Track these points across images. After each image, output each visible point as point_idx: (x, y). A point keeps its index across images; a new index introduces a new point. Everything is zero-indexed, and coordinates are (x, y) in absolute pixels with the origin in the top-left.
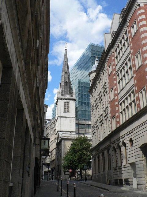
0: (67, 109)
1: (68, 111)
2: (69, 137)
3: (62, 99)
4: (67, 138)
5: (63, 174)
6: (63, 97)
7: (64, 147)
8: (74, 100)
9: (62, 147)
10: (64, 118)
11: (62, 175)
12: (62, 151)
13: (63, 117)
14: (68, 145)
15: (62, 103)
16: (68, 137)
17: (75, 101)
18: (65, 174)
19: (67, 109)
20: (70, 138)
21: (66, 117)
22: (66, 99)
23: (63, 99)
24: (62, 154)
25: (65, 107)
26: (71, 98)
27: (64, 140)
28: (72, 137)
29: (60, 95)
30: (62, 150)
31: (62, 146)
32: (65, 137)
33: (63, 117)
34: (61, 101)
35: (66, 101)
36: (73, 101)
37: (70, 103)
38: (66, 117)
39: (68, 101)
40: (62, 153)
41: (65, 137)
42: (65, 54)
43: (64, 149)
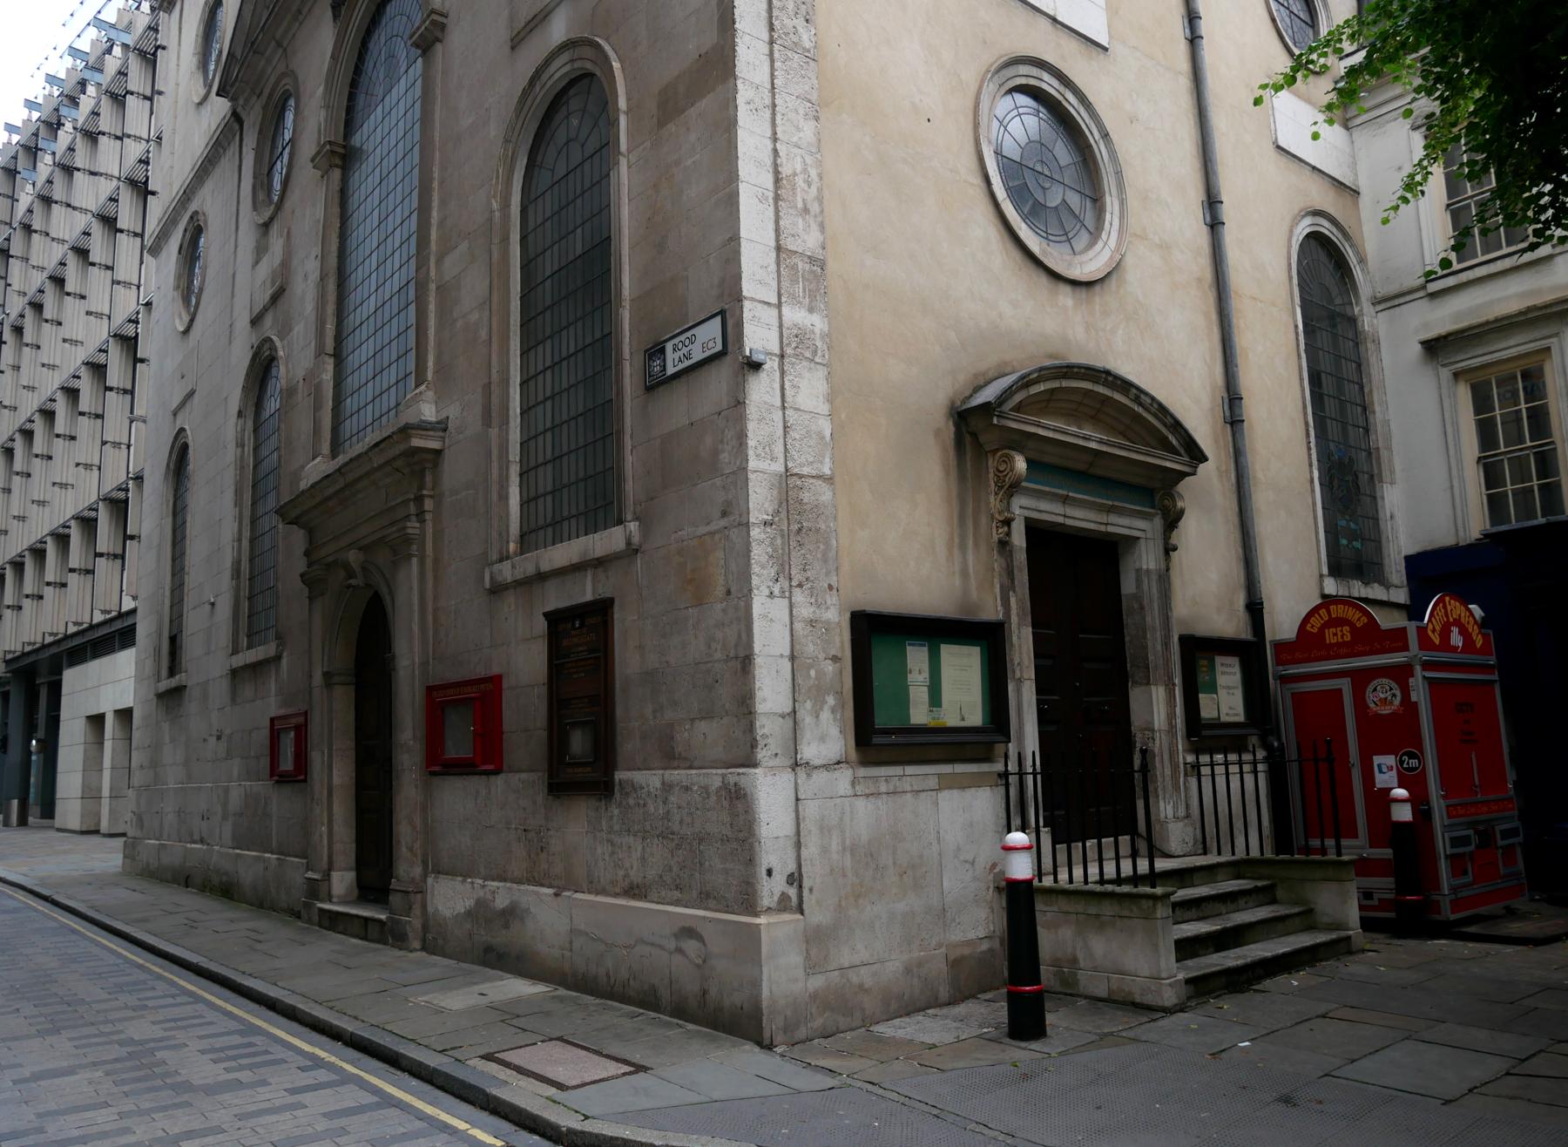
5: (828, 736)
11: (771, 796)
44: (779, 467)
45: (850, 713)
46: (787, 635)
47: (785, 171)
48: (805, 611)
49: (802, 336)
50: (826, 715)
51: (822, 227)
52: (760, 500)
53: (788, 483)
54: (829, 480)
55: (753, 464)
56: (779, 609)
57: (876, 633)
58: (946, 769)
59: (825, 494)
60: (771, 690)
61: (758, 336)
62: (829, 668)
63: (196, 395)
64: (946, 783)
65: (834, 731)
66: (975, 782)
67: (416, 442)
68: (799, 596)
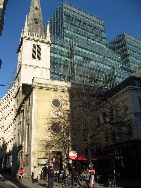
1: (39, 58)
2: (47, 84)
3: (29, 39)
4: (44, 86)
6: (31, 37)
7: (36, 105)
8: (47, 43)
10: (32, 68)
13: (30, 66)
16: (45, 84)
21: (35, 67)
22: (35, 41)
23: (32, 40)
25: (34, 52)
26: (43, 40)
29: (27, 34)
34: (28, 41)
37: (41, 47)
39: (39, 44)
41: (40, 84)
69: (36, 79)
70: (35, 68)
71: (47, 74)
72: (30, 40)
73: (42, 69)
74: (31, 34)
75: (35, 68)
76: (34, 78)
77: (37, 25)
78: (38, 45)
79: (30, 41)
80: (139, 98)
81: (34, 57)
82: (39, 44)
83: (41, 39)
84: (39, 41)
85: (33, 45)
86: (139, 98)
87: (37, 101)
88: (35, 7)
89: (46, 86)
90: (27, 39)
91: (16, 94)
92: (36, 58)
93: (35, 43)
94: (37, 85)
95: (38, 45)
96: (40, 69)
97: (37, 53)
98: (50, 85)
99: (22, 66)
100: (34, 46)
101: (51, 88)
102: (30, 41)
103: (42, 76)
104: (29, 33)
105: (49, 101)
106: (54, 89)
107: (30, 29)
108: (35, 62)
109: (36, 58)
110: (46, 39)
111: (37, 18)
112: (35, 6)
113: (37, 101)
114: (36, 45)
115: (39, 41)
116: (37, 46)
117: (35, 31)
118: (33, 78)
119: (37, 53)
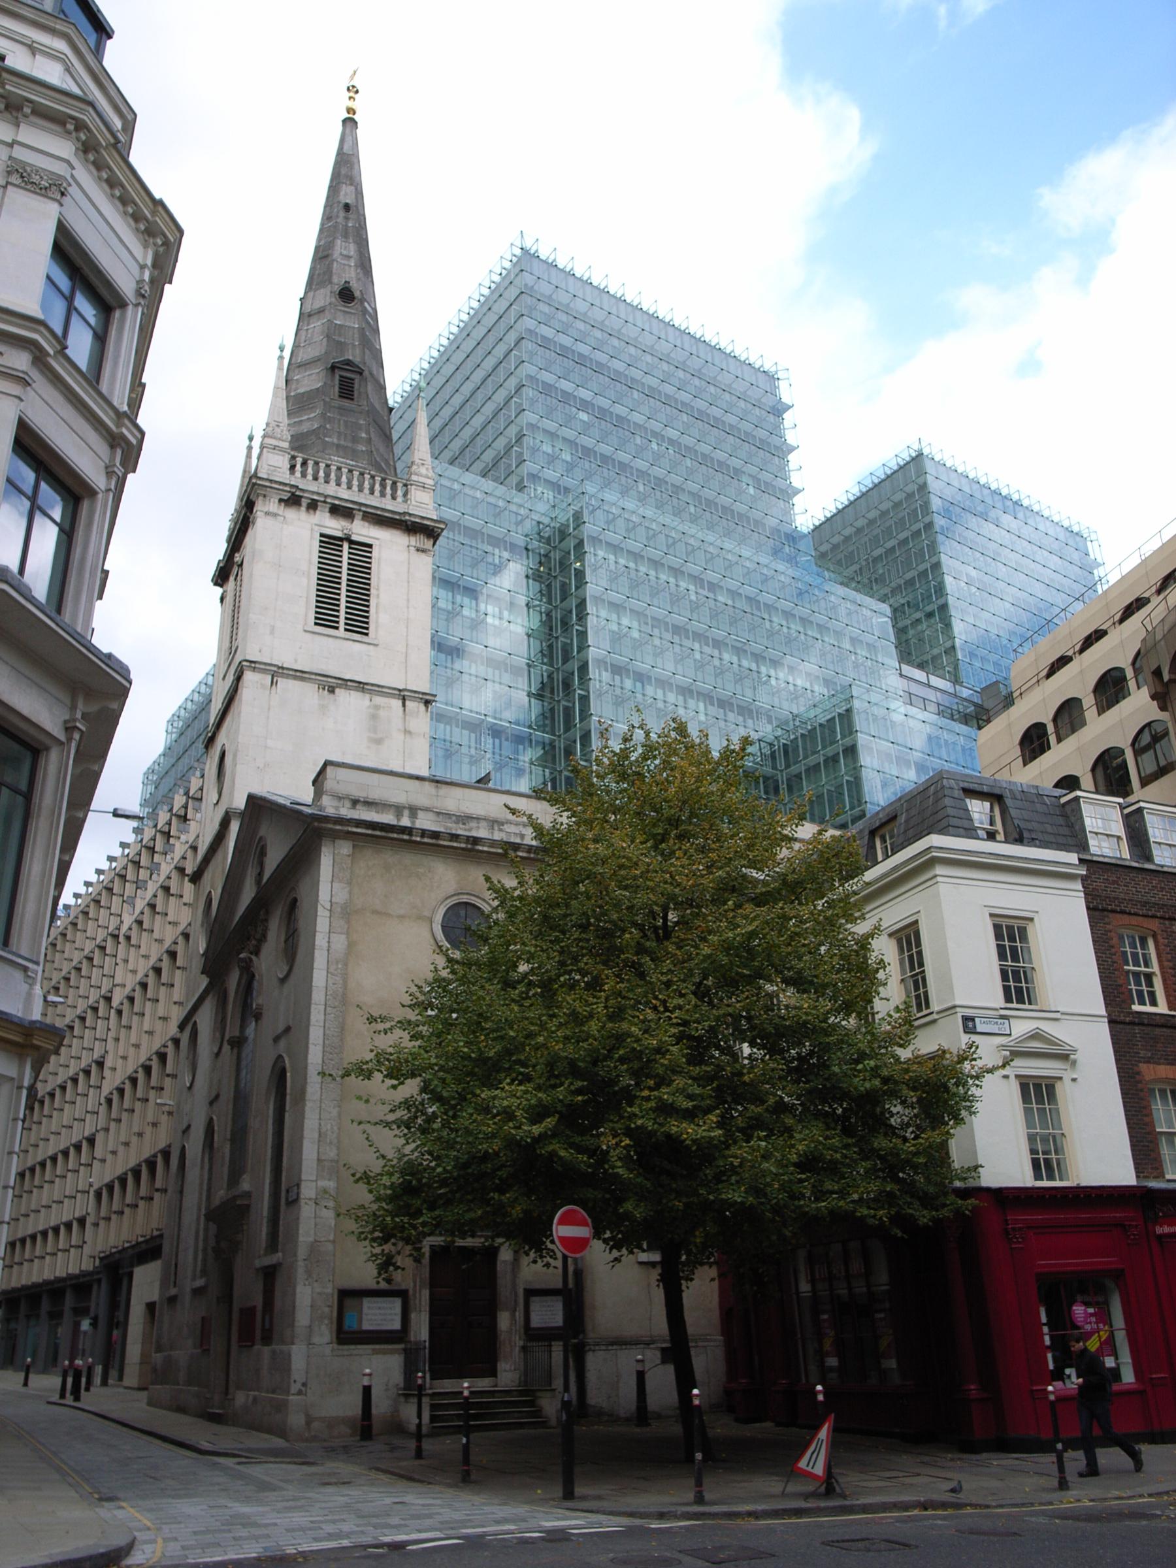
0: (343, 598)
1: (359, 624)
2: (413, 811)
3: (293, 500)
4: (388, 818)
5: (324, 1335)
6: (309, 485)
7: (339, 942)
9: (320, 940)
10: (309, 693)
12: (318, 996)
13: (300, 675)
14: (374, 958)
15: (289, 545)
16: (398, 810)
17: (428, 544)
18: (347, 1336)
19: (343, 598)
20: (425, 822)
21: (331, 684)
22: (339, 511)
23: (313, 506)
24: (316, 1034)
25: (327, 581)
26: (388, 504)
27: (345, 848)
28: (465, 819)
30: (319, 978)
31: (322, 923)
32: (369, 804)
33: (300, 675)
34: (291, 513)
35: (335, 526)
36: (414, 540)
37: (375, 554)
38: (331, 684)
39: (361, 530)
40: (317, 1015)
41: (369, 804)
42: (340, 153)
43: (343, 965)
44: (311, 1239)
45: (335, 1326)
46: (308, 1299)
47: (323, 1130)
48: (318, 1290)
49: (325, 1191)
50: (323, 1327)
51: (338, 1148)
52: (302, 1253)
53: (314, 1247)
54: (334, 1242)
55: (301, 1239)
56: (308, 1290)
57: (348, 1296)
58: (377, 1347)
59: (330, 1247)
60: (303, 1317)
61: (308, 1191)
62: (327, 1310)
63: (193, 1129)
64: (375, 1352)
65: (327, 1333)
66: (392, 1352)
67: (239, 1202)
68: (316, 1284)
69: (342, 773)
70: (332, 690)
71: (407, 732)
72: (304, 502)
73: (378, 700)
74: (310, 463)
75: (332, 690)
76: (329, 769)
77: (346, 403)
78: (351, 542)
79: (303, 509)
80: (991, 915)
81: (325, 618)
82: (361, 530)
83: (374, 501)
84: (359, 516)
85: (322, 535)
86: (991, 915)
87: (347, 913)
88: (338, 281)
89: (405, 822)
90: (281, 500)
91: (202, 849)
92: (342, 626)
93: (335, 526)
94: (346, 812)
95: (354, 538)
96: (367, 696)
97: (343, 592)
98: (431, 816)
99: (249, 676)
100: (330, 543)
101: (435, 835)
102: (303, 509)
103: (379, 742)
104: (299, 460)
105: (420, 918)
106: (455, 837)
107: (305, 428)
108: (336, 653)
109: (342, 626)
110: (405, 501)
111: (348, 362)
112: (335, 280)
113: (347, 913)
114: (341, 539)
115: (359, 516)
116: (346, 545)
117: (338, 446)
118: (327, 764)
119: (343, 592)
